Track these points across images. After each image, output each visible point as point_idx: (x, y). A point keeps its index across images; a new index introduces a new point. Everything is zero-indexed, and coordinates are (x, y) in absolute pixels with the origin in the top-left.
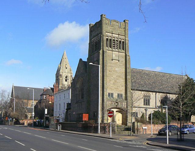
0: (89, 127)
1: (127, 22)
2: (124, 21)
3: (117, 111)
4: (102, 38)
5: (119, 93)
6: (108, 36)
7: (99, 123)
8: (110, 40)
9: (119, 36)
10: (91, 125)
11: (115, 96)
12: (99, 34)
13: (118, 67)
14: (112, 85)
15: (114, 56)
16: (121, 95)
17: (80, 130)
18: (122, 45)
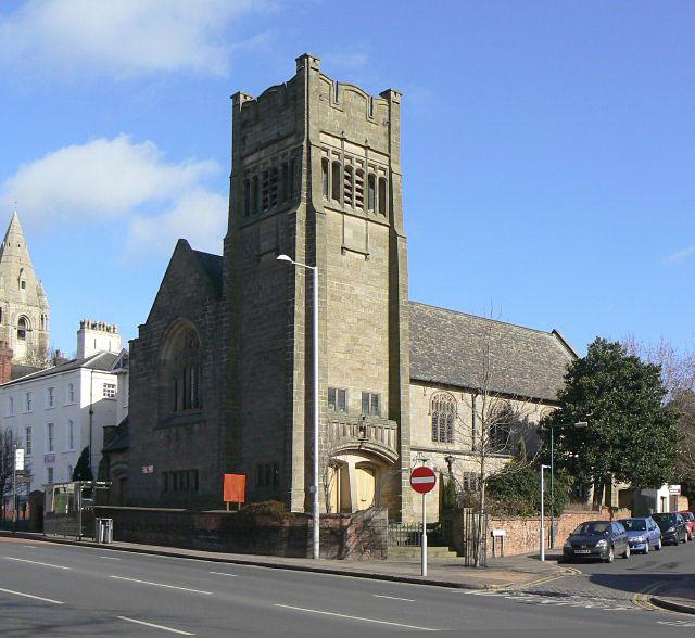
0: (264, 528)
1: (398, 99)
2: (386, 94)
3: (358, 466)
4: (305, 156)
5: (368, 390)
6: (327, 150)
7: (317, 515)
8: (336, 165)
9: (366, 154)
10: (275, 523)
11: (354, 401)
12: (288, 136)
13: (365, 283)
14: (342, 356)
15: (348, 233)
16: (376, 398)
17: (210, 541)
18: (379, 193)
